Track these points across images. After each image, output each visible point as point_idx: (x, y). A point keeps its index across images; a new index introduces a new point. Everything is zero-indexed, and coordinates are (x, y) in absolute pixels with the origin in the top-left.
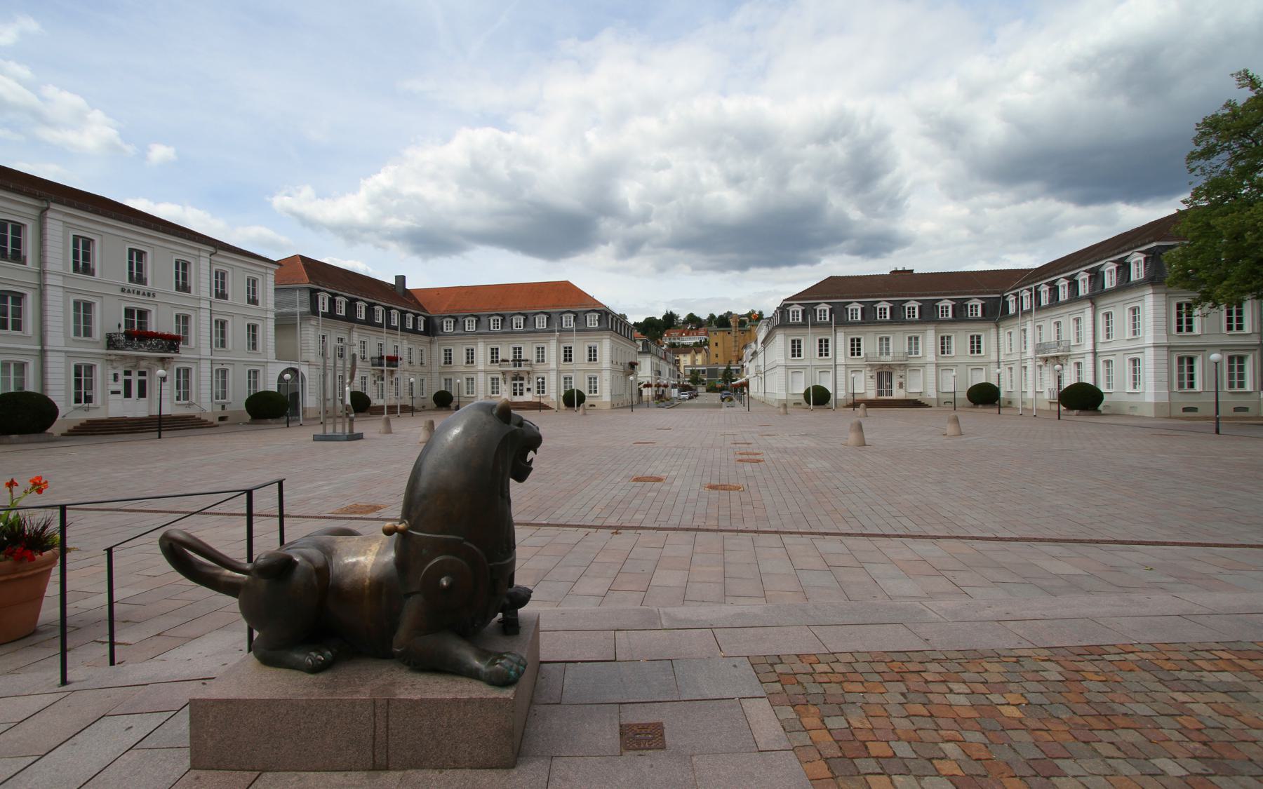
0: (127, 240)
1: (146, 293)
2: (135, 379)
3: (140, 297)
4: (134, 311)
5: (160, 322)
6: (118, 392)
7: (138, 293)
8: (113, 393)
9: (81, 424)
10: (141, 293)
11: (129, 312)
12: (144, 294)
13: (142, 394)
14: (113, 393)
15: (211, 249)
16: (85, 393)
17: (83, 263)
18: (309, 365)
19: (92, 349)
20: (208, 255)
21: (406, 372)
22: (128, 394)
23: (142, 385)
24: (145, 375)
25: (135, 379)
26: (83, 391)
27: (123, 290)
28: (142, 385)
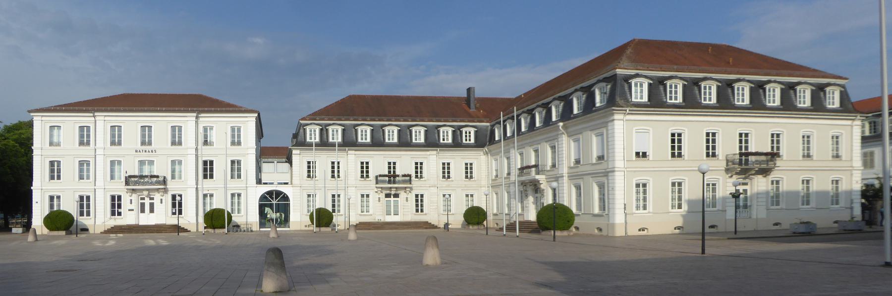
0: (138, 121)
1: (150, 151)
2: (147, 202)
3: (147, 153)
4: (207, 161)
5: (161, 168)
6: (133, 210)
7: (146, 151)
8: (129, 210)
9: (112, 228)
10: (147, 151)
11: (142, 163)
12: (149, 152)
13: (152, 210)
14: (129, 210)
15: (195, 114)
16: (118, 210)
17: (118, 140)
18: (292, 187)
19: (119, 187)
20: (194, 119)
21: (431, 188)
22: (143, 211)
23: (152, 205)
24: (153, 199)
25: (147, 202)
26: (116, 209)
27: (136, 151)
28: (152, 205)
